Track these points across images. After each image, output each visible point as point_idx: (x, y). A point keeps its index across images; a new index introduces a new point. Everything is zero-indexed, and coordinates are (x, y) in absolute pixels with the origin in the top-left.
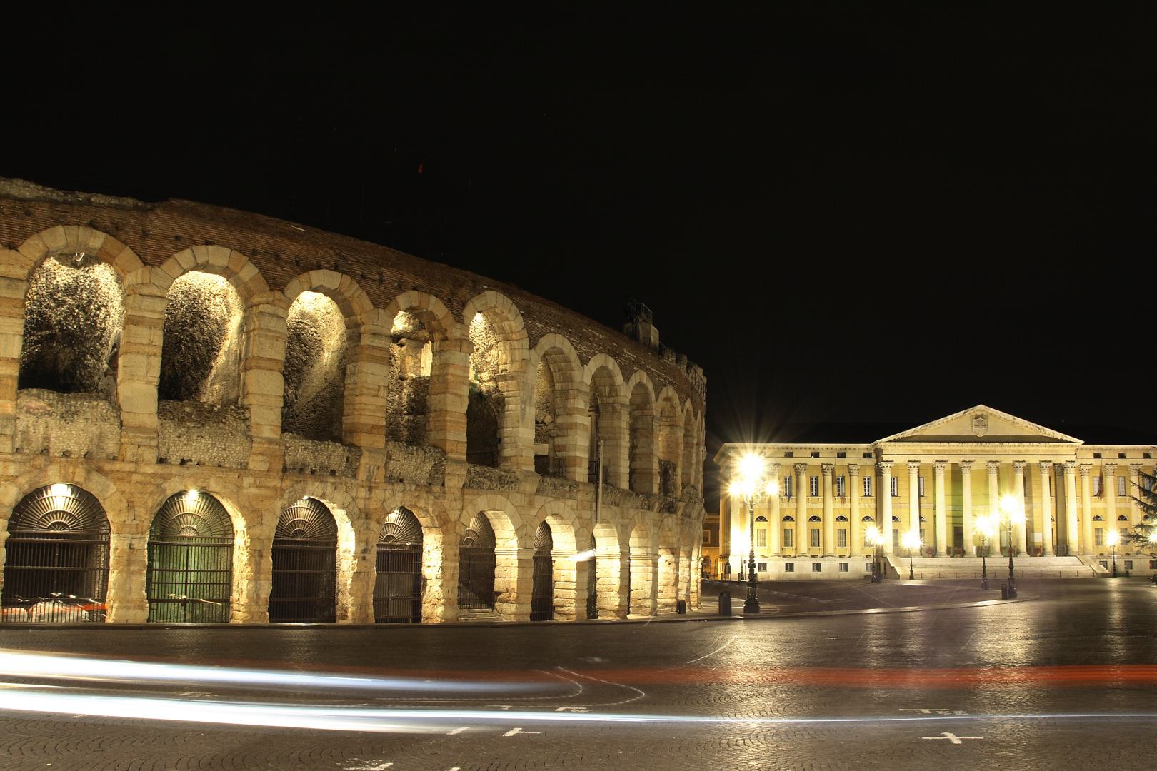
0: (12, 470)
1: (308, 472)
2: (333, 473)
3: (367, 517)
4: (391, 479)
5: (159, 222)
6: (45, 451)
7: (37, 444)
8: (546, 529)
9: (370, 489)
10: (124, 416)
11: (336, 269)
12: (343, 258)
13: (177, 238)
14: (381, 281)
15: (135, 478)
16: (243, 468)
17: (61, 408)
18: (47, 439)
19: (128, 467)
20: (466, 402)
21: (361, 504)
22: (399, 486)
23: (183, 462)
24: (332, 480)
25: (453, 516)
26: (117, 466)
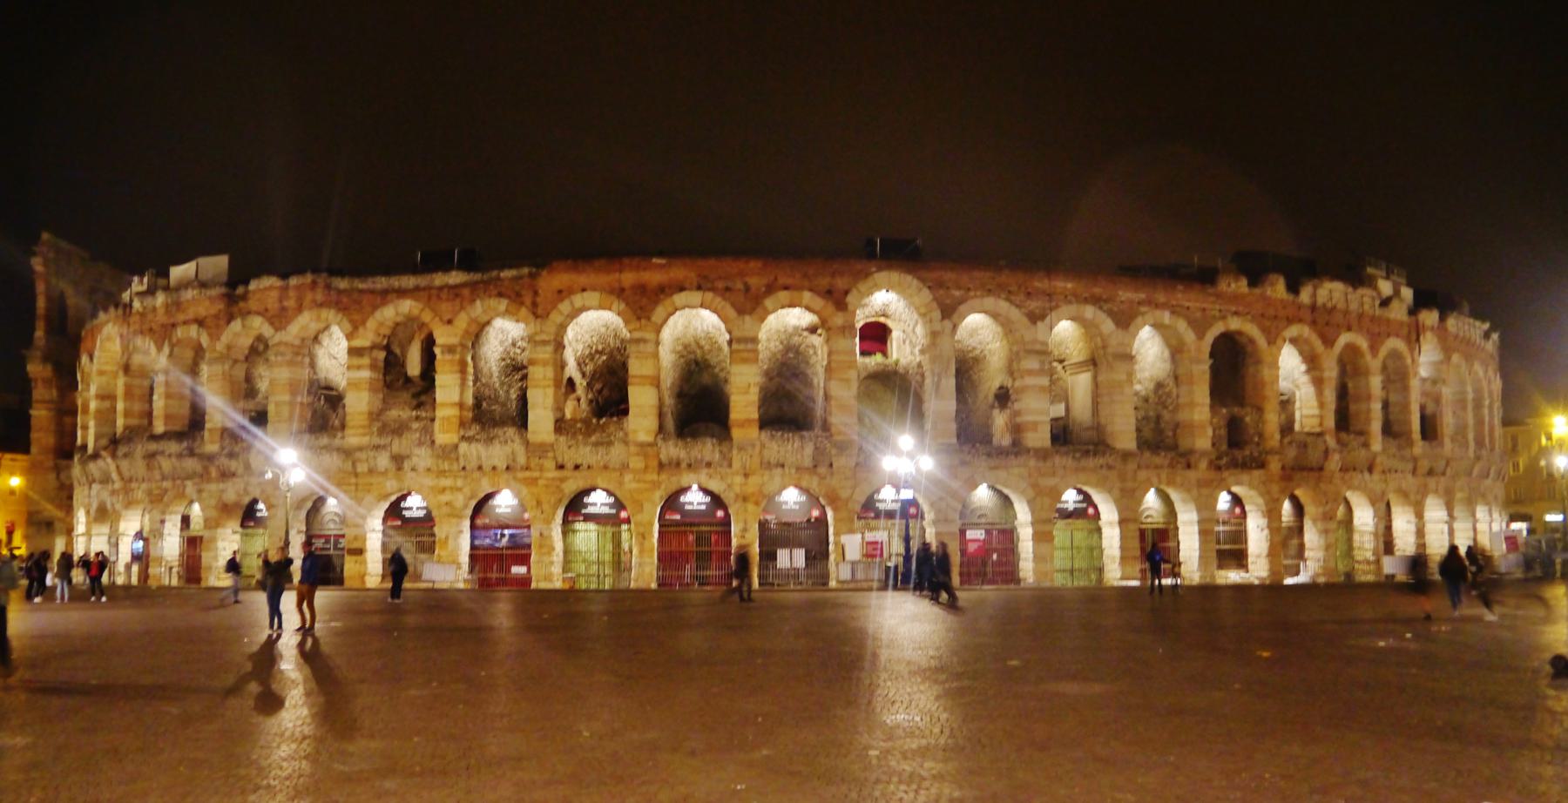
0: (459, 483)
1: (684, 465)
2: (709, 465)
3: (745, 499)
4: (767, 466)
5: (551, 281)
6: (480, 468)
7: (473, 464)
8: (1006, 501)
9: (746, 475)
10: (530, 436)
11: (699, 288)
12: (705, 278)
13: (560, 292)
14: (747, 289)
15: (541, 482)
16: (625, 467)
17: (484, 436)
18: (479, 458)
19: (536, 474)
20: (855, 385)
21: (737, 489)
22: (779, 470)
23: (577, 467)
24: (705, 471)
25: (844, 494)
26: (527, 474)
